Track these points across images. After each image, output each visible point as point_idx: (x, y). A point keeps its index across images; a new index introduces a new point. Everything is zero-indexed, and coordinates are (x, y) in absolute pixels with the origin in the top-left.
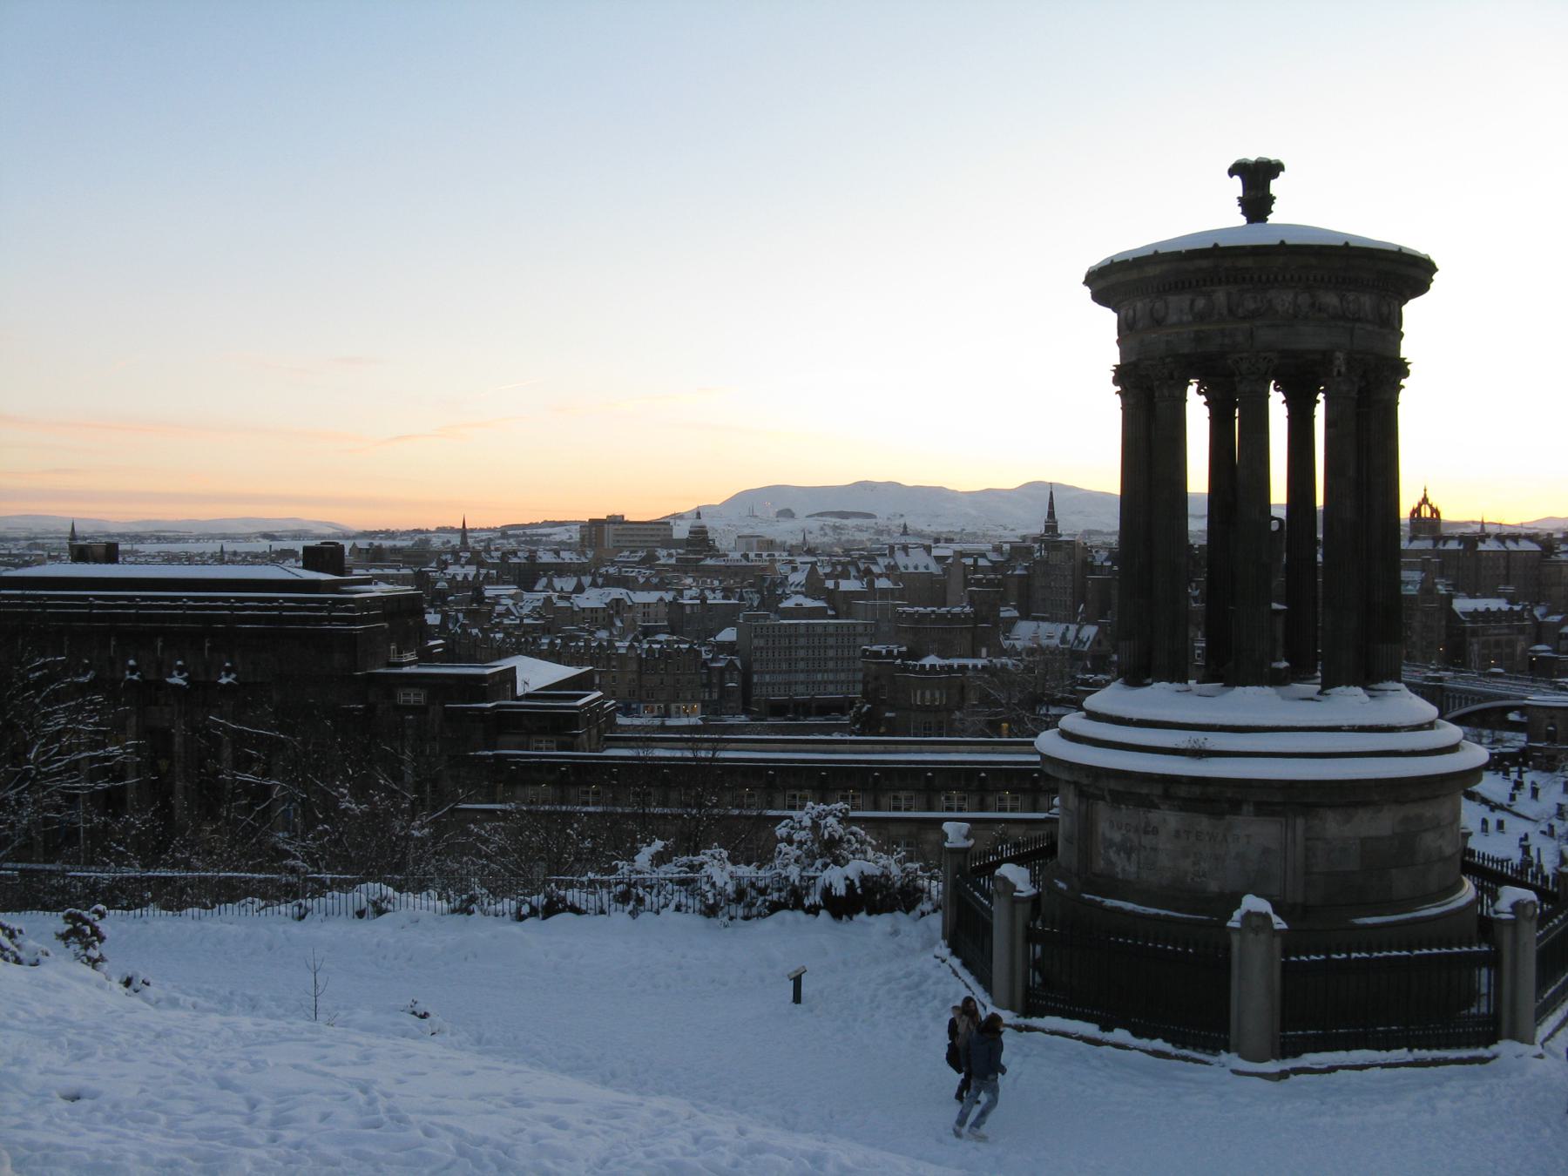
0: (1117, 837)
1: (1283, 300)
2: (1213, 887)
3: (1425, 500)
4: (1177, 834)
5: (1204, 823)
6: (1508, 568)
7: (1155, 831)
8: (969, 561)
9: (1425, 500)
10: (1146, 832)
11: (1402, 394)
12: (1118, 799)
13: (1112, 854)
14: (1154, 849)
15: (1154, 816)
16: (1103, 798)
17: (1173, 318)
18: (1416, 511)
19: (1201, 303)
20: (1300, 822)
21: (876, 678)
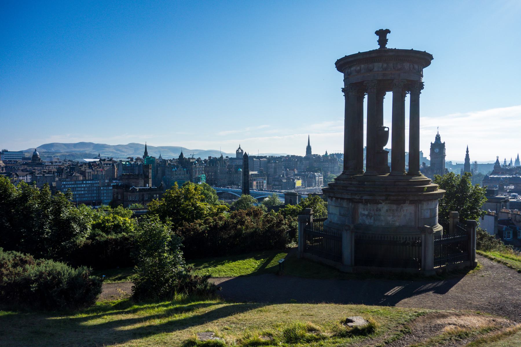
0: (366, 213)
1: (407, 65)
2: (397, 224)
3: (240, 148)
4: (387, 211)
5: (394, 207)
6: (260, 164)
7: (380, 210)
8: (124, 163)
9: (240, 148)
10: (377, 211)
11: (421, 95)
12: (367, 202)
13: (364, 217)
14: (379, 215)
15: (380, 206)
16: (362, 202)
17: (375, 69)
18: (238, 151)
19: (385, 65)
20: (420, 205)
21: (117, 193)
